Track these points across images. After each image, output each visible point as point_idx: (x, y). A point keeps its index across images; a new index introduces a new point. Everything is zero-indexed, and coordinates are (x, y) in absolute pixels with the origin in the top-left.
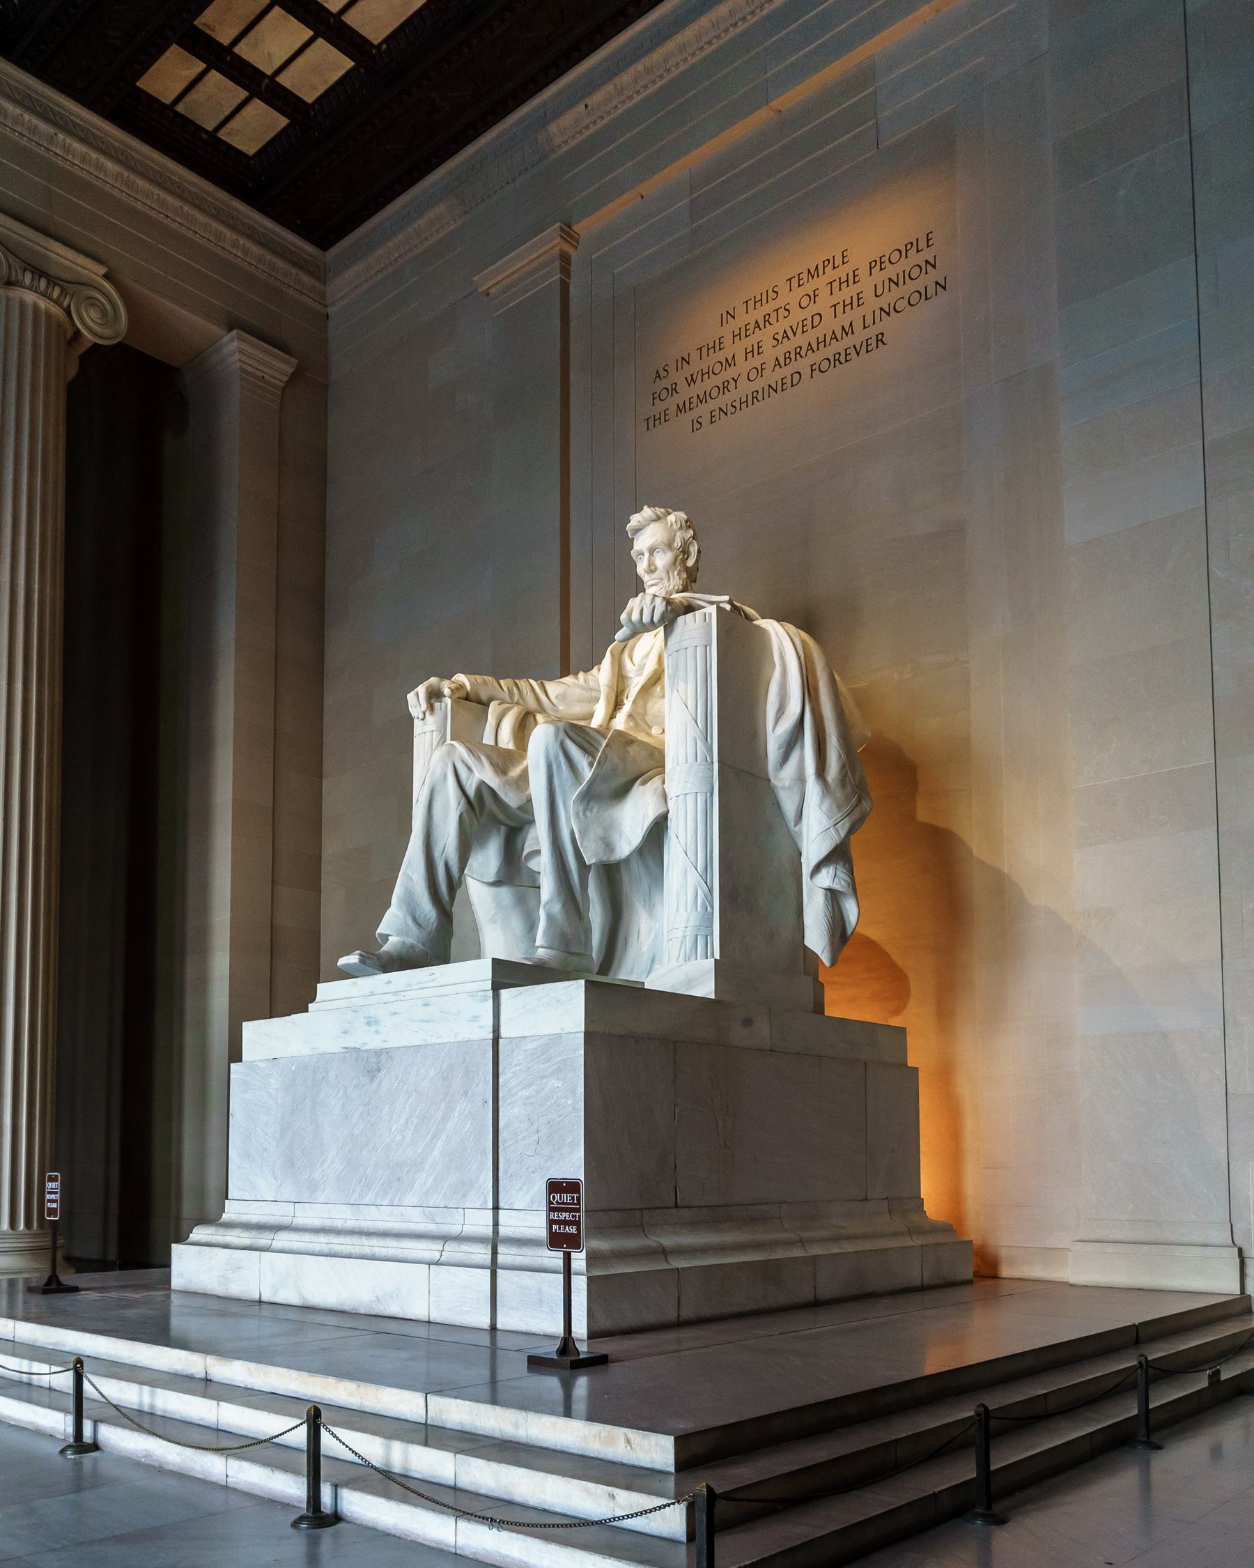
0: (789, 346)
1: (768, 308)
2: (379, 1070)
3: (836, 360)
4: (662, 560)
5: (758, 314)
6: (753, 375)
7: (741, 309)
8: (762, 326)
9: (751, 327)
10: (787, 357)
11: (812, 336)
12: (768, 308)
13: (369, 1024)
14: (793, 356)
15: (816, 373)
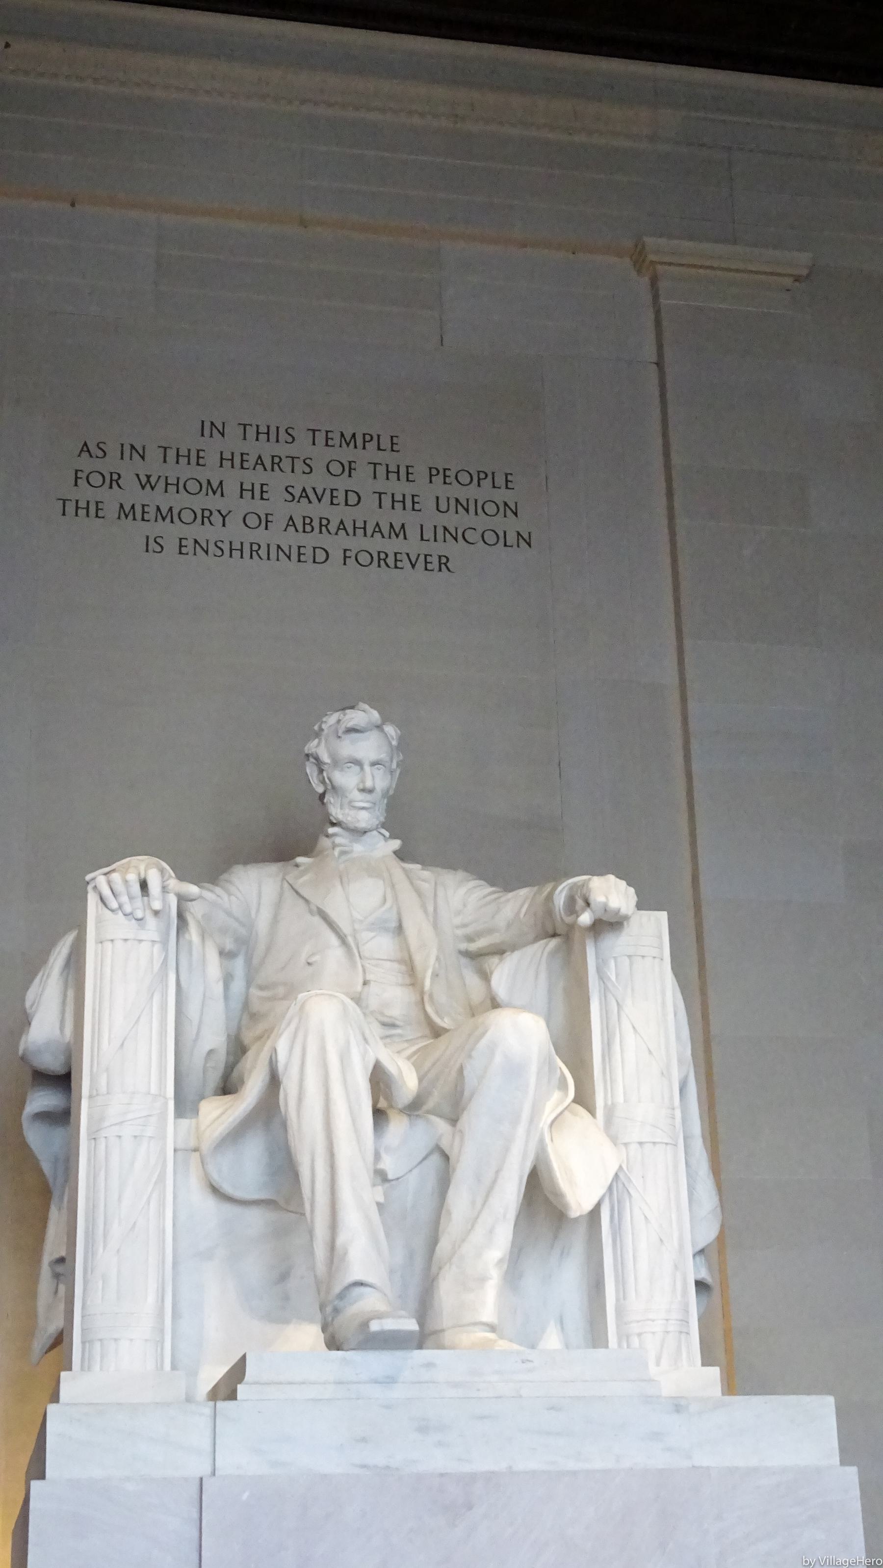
0: (317, 510)
1: (283, 450)
2: (470, 1507)
3: (381, 559)
4: (380, 781)
5: (267, 450)
6: (252, 521)
7: (233, 431)
8: (268, 465)
9: (252, 459)
10: (308, 522)
11: (349, 515)
12: (283, 450)
13: (424, 1429)
14: (316, 523)
15: (351, 562)
